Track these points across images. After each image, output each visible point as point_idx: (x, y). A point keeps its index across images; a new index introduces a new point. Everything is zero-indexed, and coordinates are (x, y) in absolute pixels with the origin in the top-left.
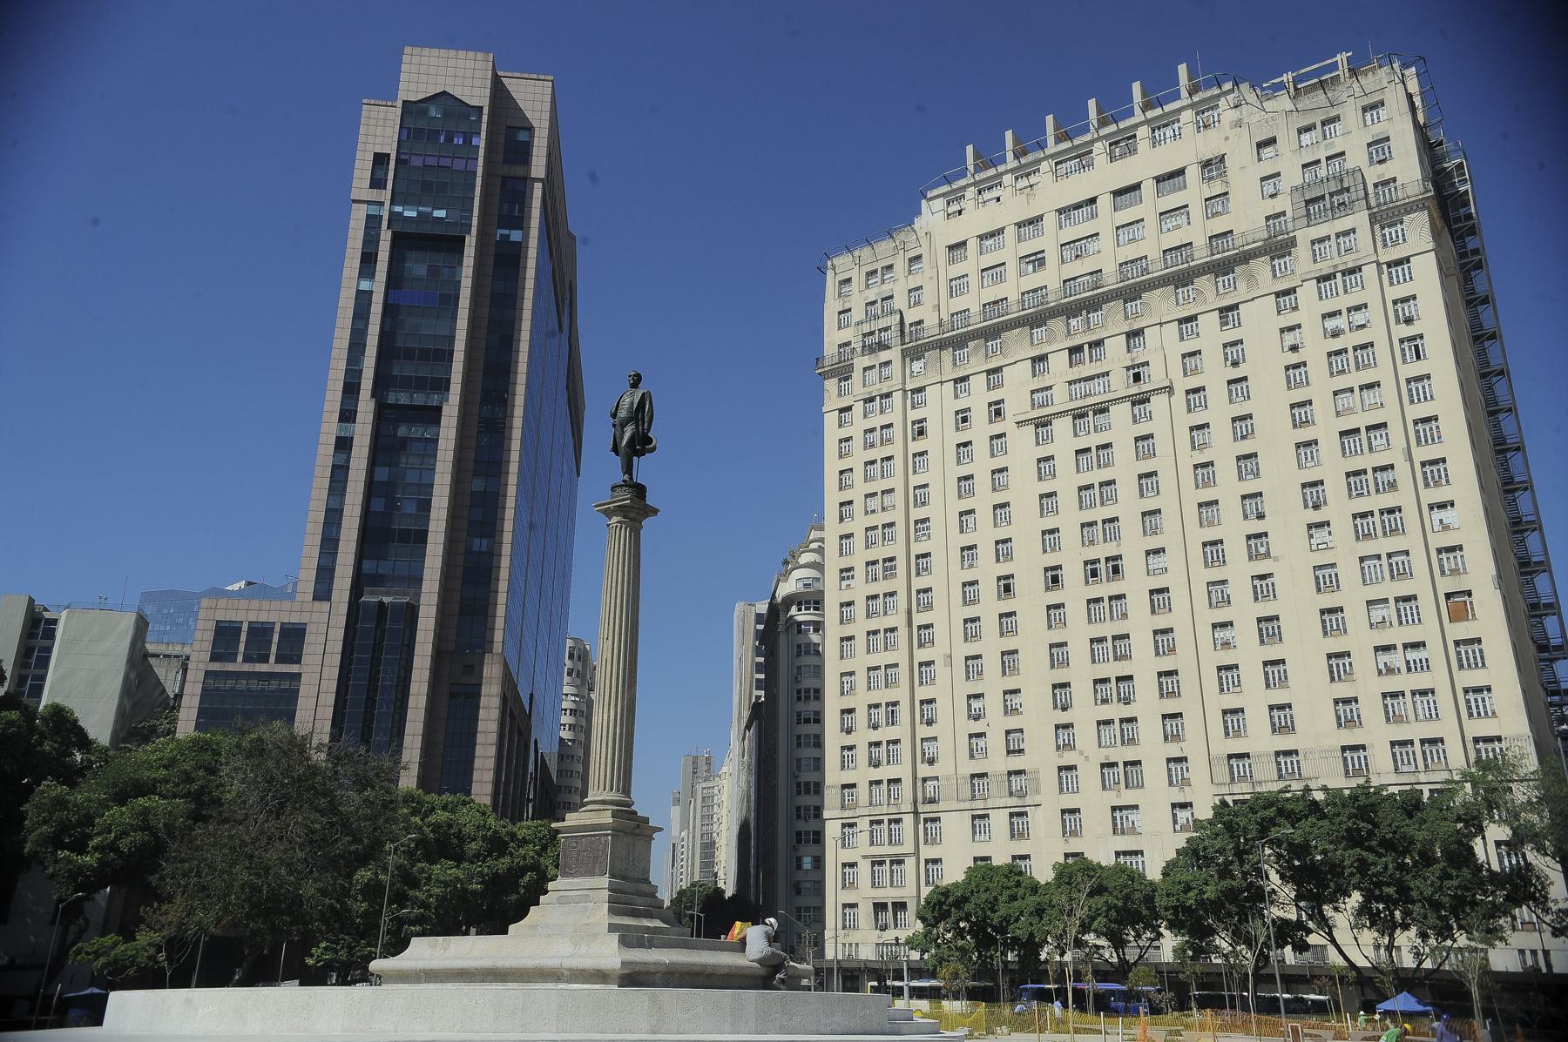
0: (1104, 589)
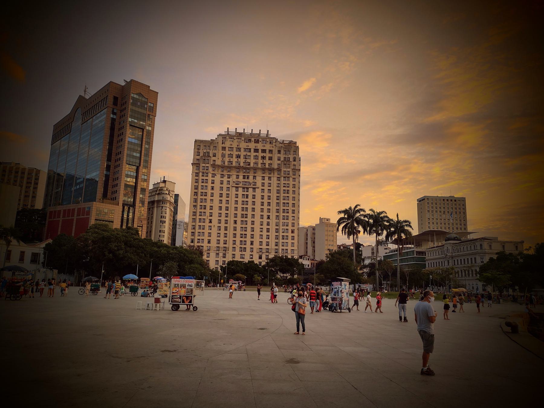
0: (244, 219)
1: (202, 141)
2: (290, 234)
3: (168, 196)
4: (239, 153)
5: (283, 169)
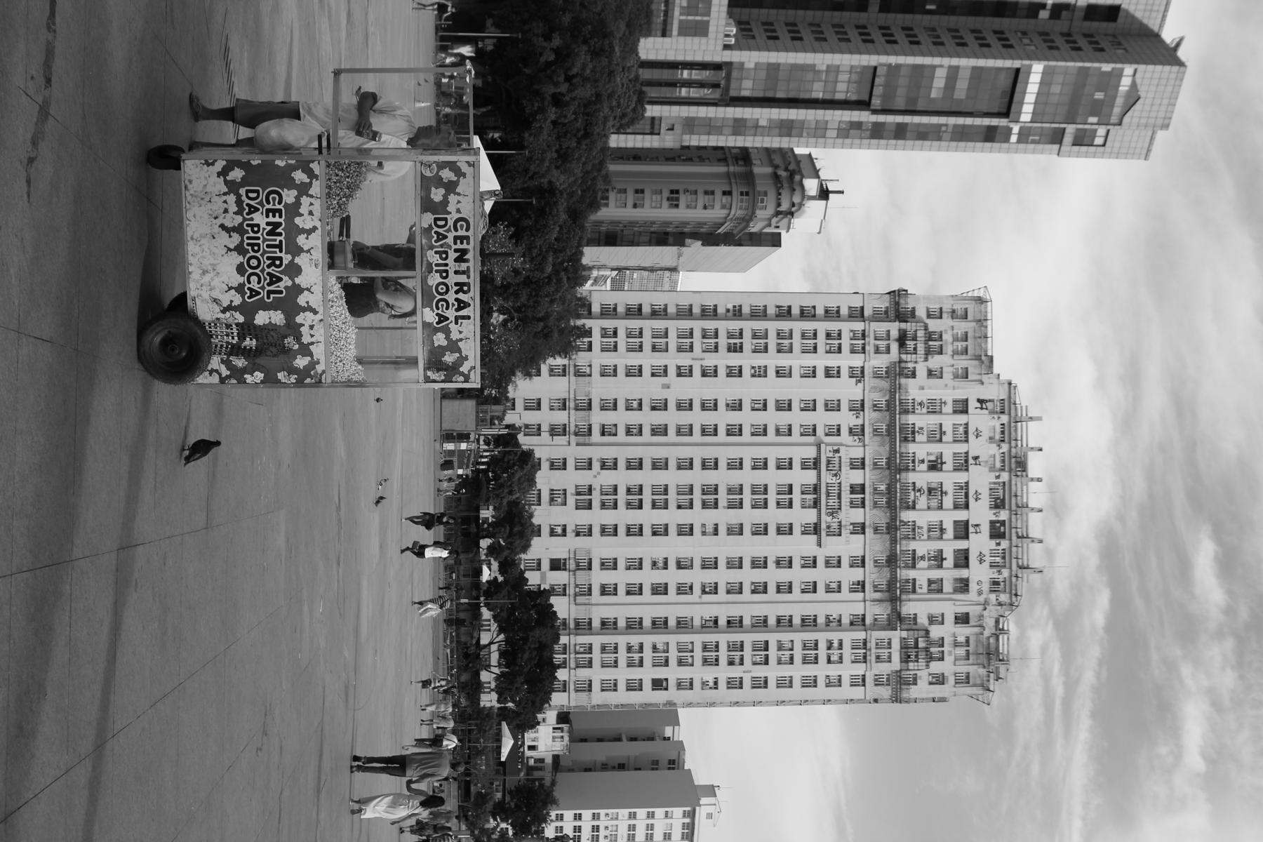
0: (697, 497)
1: (982, 322)
2: (647, 674)
3: (770, 210)
4: (948, 466)
5: (896, 636)
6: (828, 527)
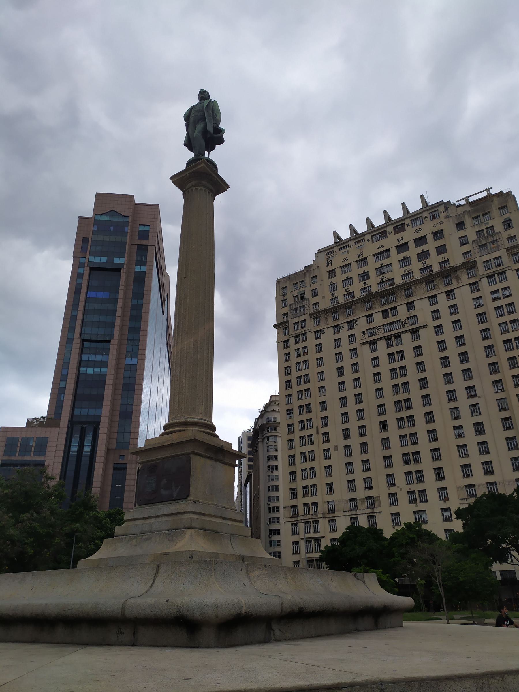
0: (404, 414)
6: (412, 324)
